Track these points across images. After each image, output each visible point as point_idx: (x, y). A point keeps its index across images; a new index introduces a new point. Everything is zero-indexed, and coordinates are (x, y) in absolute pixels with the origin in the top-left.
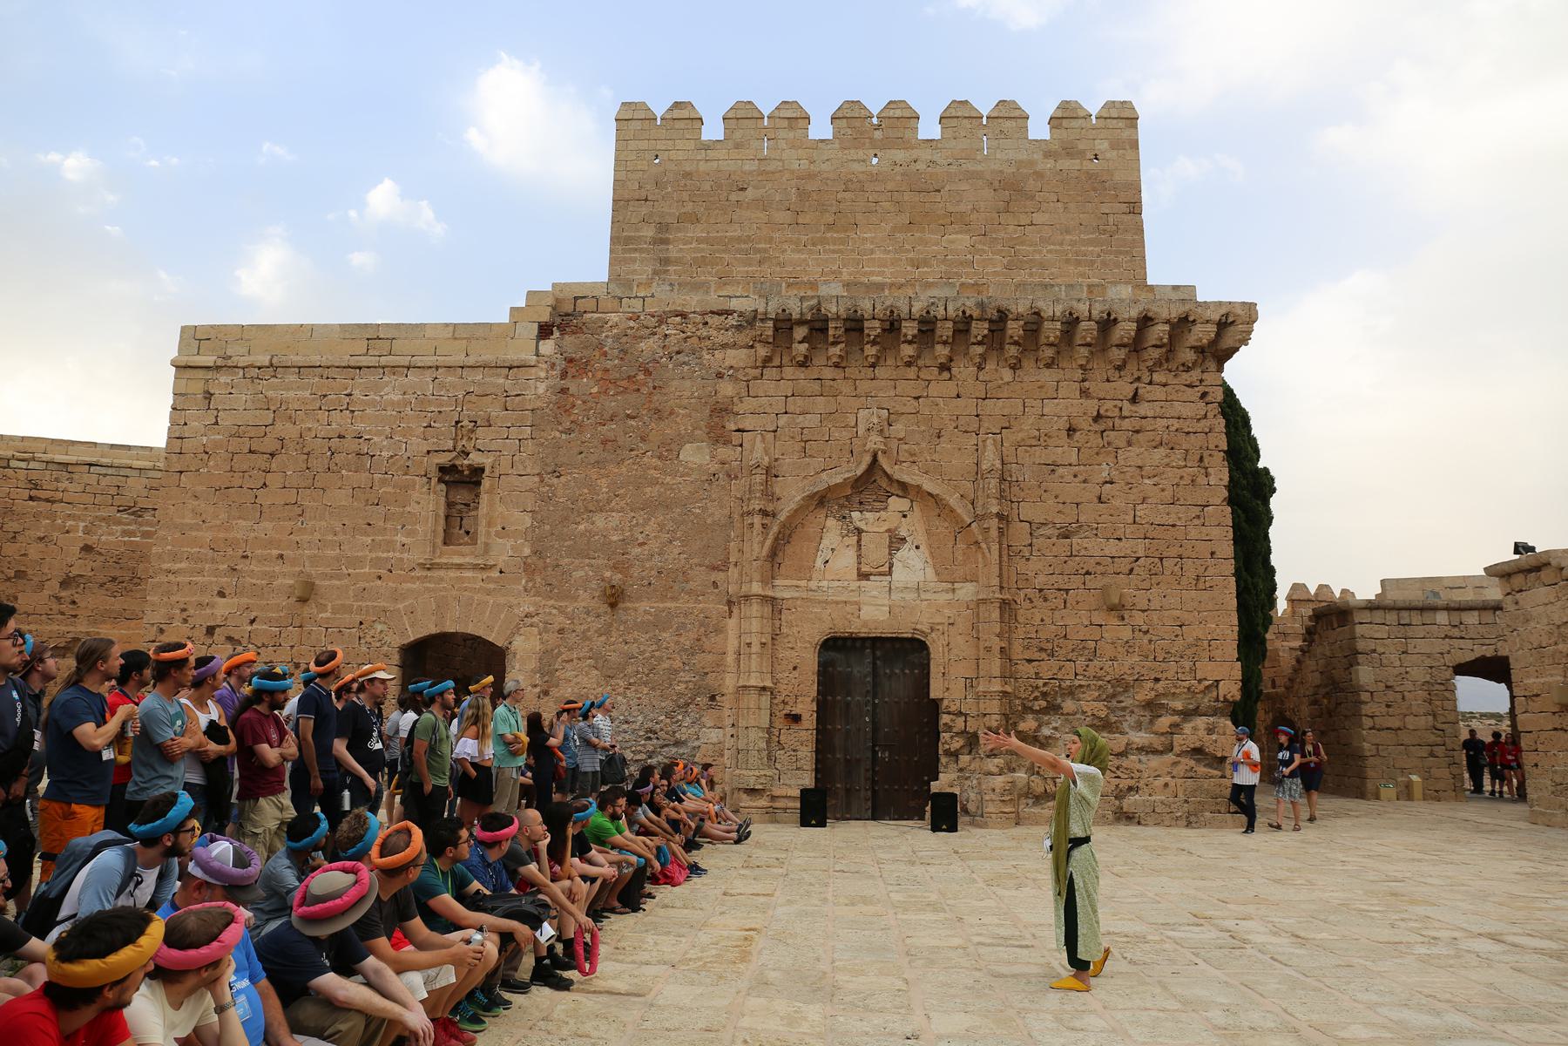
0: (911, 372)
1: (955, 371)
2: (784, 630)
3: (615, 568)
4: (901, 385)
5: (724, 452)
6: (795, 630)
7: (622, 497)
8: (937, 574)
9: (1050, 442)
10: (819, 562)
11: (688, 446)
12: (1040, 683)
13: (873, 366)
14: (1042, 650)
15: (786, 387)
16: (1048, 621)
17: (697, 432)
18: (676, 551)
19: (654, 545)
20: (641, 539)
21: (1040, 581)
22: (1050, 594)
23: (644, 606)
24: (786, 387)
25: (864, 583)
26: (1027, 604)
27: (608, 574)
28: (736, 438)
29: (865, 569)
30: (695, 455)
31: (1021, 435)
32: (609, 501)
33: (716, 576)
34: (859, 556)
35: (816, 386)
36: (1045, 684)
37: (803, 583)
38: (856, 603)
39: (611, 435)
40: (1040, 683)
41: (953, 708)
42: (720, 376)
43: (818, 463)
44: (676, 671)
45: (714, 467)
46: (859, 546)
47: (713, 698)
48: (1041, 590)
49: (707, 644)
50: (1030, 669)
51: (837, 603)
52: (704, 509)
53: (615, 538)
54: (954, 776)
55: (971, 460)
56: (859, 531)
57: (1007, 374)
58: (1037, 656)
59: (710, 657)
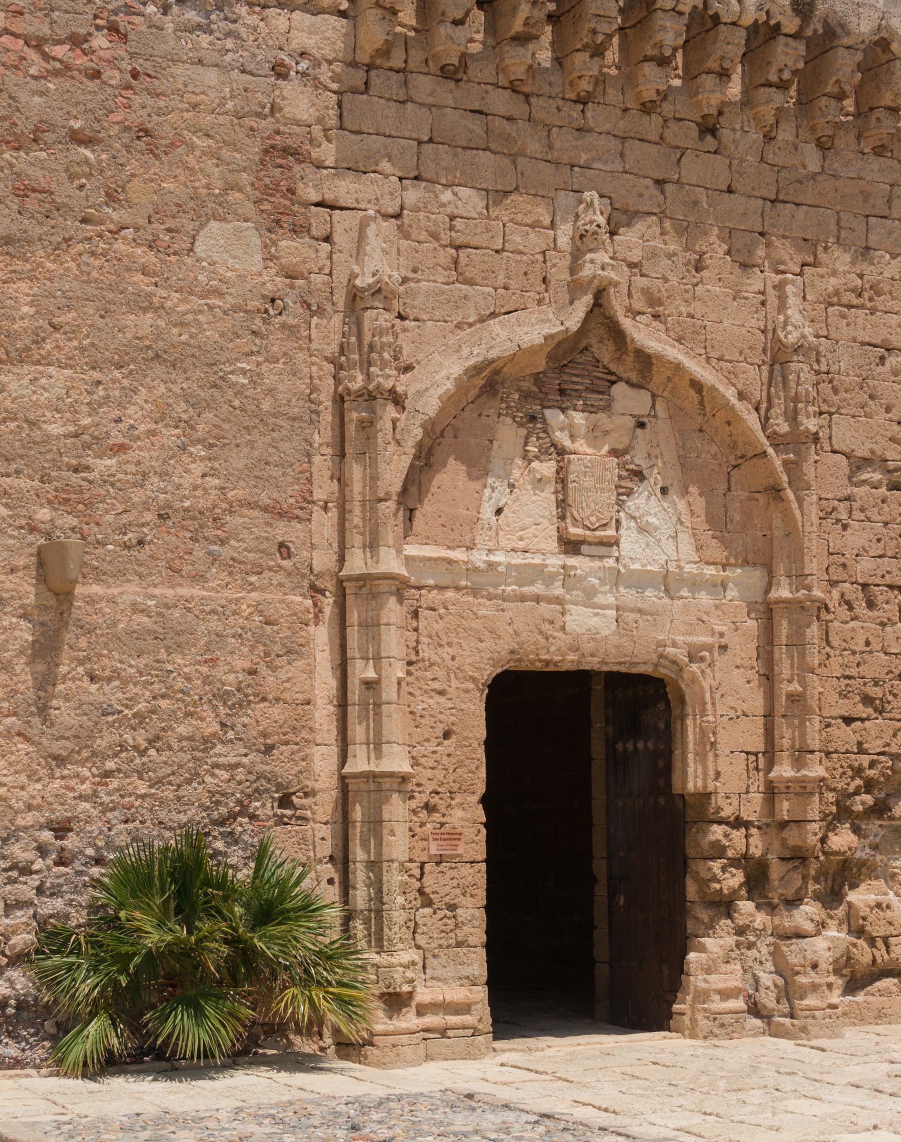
0: (651, 126)
1: (725, 134)
2: (426, 652)
3: (61, 501)
4: (635, 149)
5: (291, 248)
6: (446, 653)
7: (73, 332)
8: (699, 548)
9: (879, 301)
10: (487, 512)
11: (214, 225)
12: (865, 760)
13: (583, 101)
14: (867, 700)
15: (418, 121)
16: (876, 645)
17: (235, 196)
18: (198, 469)
19: (144, 454)
20: (117, 438)
21: (864, 567)
22: (881, 594)
23: (130, 591)
24: (418, 121)
25: (572, 561)
26: (843, 612)
27: (44, 514)
28: (318, 219)
29: (575, 531)
30: (232, 251)
31: (833, 282)
32: (39, 342)
33: (282, 531)
34: (562, 504)
35: (476, 125)
36: (872, 765)
37: (458, 555)
38: (558, 601)
39: (38, 176)
40: (865, 760)
41: (727, 812)
42: (280, 71)
43: (481, 296)
44: (208, 742)
45: (274, 283)
46: (562, 479)
47: (285, 801)
48: (865, 586)
49: (270, 681)
50: (845, 736)
51: (523, 599)
52: (255, 379)
53: (55, 429)
54: (731, 940)
55: (756, 322)
56: (562, 452)
57: (812, 160)
58: (861, 710)
59: (276, 712)
